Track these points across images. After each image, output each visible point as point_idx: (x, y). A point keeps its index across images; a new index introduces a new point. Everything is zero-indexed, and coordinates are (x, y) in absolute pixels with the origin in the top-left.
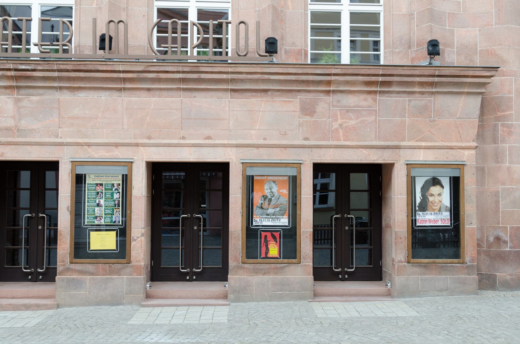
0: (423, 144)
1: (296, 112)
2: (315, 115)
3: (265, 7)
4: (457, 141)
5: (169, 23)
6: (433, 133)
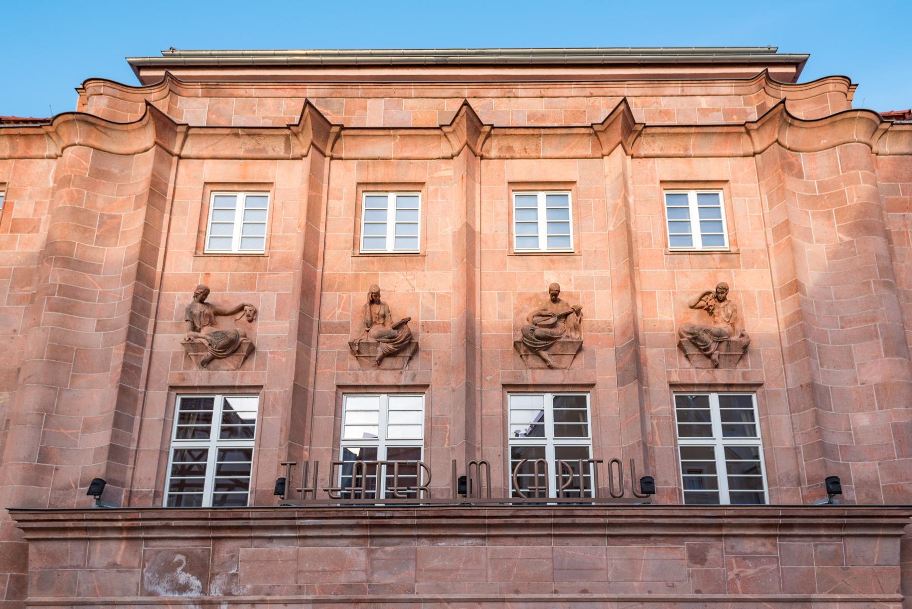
0: (838, 596)
1: (684, 559)
2: (706, 563)
3: (634, 444)
4: (878, 593)
5: (536, 463)
6: (848, 583)
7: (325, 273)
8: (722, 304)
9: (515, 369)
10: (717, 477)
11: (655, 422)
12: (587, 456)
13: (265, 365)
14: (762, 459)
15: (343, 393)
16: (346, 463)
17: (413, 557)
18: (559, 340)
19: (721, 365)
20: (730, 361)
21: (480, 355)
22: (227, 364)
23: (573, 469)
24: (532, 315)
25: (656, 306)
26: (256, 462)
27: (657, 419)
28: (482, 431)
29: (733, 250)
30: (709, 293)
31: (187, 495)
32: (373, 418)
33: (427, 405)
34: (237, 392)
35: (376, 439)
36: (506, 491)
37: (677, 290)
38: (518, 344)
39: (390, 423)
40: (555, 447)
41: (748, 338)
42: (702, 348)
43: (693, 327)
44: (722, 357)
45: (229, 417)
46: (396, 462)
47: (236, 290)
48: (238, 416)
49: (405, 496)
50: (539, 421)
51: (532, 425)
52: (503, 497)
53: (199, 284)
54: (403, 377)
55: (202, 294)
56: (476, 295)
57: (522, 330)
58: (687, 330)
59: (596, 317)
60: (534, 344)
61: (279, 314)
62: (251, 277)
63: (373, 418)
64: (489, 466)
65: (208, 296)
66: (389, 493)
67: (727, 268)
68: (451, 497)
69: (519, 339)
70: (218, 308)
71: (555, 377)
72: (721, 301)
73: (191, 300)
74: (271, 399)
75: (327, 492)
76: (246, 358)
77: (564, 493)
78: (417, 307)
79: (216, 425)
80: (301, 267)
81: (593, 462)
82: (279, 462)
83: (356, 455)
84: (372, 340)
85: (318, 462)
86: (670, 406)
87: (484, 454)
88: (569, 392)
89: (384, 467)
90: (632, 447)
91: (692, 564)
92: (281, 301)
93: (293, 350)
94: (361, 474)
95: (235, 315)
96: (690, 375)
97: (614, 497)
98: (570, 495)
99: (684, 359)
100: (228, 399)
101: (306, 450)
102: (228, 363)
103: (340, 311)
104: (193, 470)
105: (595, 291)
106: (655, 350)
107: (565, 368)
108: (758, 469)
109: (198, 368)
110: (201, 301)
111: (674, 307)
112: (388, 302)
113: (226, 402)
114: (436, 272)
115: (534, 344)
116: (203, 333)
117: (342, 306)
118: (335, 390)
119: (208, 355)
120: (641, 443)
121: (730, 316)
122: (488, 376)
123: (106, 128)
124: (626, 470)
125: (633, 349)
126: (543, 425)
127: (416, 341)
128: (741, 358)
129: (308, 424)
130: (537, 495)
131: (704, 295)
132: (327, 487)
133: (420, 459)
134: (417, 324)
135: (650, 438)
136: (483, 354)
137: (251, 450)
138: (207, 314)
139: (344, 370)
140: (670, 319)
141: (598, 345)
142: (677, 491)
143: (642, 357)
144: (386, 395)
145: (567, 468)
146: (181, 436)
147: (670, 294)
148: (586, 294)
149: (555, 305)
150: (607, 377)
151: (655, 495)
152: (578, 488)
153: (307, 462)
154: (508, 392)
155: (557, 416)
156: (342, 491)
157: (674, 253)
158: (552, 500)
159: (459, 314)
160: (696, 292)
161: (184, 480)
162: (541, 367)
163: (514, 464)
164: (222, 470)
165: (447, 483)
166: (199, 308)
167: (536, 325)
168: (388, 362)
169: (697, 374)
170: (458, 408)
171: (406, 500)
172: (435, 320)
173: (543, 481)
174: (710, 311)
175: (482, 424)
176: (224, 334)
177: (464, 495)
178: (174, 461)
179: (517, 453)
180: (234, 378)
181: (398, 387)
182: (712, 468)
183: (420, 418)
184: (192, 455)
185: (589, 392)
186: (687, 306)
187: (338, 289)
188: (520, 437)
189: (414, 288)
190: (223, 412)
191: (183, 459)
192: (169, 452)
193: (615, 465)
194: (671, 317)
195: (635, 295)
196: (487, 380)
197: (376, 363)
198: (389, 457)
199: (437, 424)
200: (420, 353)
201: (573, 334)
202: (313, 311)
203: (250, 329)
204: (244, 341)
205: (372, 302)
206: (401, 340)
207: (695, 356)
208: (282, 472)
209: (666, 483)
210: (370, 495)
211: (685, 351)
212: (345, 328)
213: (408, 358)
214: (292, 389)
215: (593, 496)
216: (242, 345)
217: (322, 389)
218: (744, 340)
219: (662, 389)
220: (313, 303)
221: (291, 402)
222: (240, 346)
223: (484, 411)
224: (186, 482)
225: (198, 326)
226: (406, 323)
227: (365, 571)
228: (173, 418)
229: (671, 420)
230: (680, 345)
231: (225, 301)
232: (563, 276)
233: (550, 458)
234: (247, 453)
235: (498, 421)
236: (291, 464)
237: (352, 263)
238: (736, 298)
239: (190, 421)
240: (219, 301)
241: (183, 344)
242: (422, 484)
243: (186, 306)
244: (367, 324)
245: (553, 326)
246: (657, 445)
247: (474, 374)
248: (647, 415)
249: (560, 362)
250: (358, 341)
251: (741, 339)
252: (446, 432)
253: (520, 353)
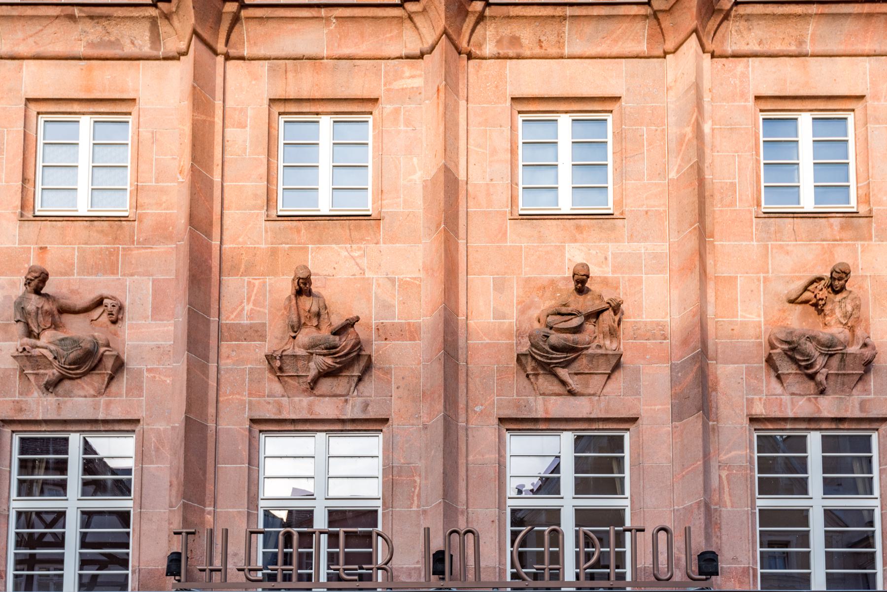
3: (691, 505)
5: (546, 533)
7: (224, 246)
8: (839, 297)
9: (517, 395)
10: (808, 531)
11: (724, 474)
12: (622, 523)
13: (140, 388)
14: (878, 528)
15: (261, 431)
16: (267, 532)
19: (829, 390)
20: (843, 384)
21: (464, 375)
22: (83, 388)
23: (600, 540)
24: (546, 314)
25: (737, 300)
26: (137, 530)
27: (728, 470)
28: (467, 486)
29: (863, 210)
30: (820, 279)
31: (40, 575)
32: (306, 467)
33: (386, 450)
34: (102, 429)
35: (310, 496)
36: (502, 572)
37: (770, 275)
38: (523, 359)
39: (331, 474)
40: (576, 510)
41: (874, 348)
42: (803, 364)
43: (791, 333)
44: (831, 378)
45: (92, 465)
46: (341, 530)
47: (89, 274)
48: (105, 463)
49: (356, 578)
50: (552, 473)
51: (541, 478)
52: (497, 580)
53: (31, 265)
54: (349, 407)
55: (36, 281)
56: (460, 282)
57: (529, 336)
58: (782, 336)
59: (644, 316)
60: (547, 358)
61: (157, 311)
62: (111, 254)
63: (306, 467)
64: (478, 537)
65: (47, 283)
66: (333, 573)
67: (851, 239)
68: (423, 580)
69: (524, 349)
70: (63, 301)
71: (579, 407)
72: (836, 292)
73: (21, 289)
74: (154, 439)
75: (242, 573)
76: (111, 378)
77: (586, 574)
78: (369, 300)
79: (74, 476)
80: (186, 237)
81: (630, 530)
82: (169, 529)
83: (282, 519)
84: (301, 352)
85: (227, 530)
86: (748, 451)
87: (470, 520)
88: (598, 429)
89: (324, 538)
90: (689, 510)
92: (158, 291)
93: (181, 366)
94: (291, 547)
95: (90, 313)
96: (781, 404)
97: (658, 579)
98: (596, 576)
99: (774, 381)
100: (88, 439)
101: (209, 513)
102: (85, 386)
103: (251, 306)
104: (46, 539)
105: (644, 276)
106: (731, 367)
107: (594, 395)
108: (871, 541)
109: (40, 393)
110: (37, 291)
111: (764, 302)
112: (325, 293)
113: (86, 442)
114: (398, 245)
115: (547, 358)
116: (44, 340)
117: (253, 298)
118: (248, 426)
119: (53, 374)
120: (702, 504)
121: (848, 314)
122: (477, 405)
124: (679, 543)
125: (697, 365)
126: (559, 478)
127: (368, 353)
128: (860, 379)
129: (210, 475)
130: (547, 576)
131: (812, 283)
132: (241, 565)
133: (377, 527)
134: (369, 327)
135: (716, 498)
136: (470, 374)
137: (128, 513)
138: (47, 312)
139: (260, 396)
140: (758, 319)
141: (644, 358)
142: (751, 571)
143: (711, 377)
144: (324, 434)
145: (591, 538)
146: (23, 492)
147: (759, 280)
148: (629, 280)
149: (581, 298)
150: (657, 407)
151: (719, 577)
152: (608, 567)
153: (211, 530)
154: (507, 430)
155: (580, 465)
156: (265, 571)
157: (769, 215)
158: (569, 584)
159: (433, 312)
160: (799, 278)
161: (34, 554)
162: (557, 392)
163: (514, 534)
164: (88, 540)
165: (416, 560)
166: (34, 303)
167: (551, 328)
168: (326, 385)
169: (792, 403)
170: (433, 452)
171: (358, 583)
172: (396, 321)
173: (556, 558)
174: (818, 307)
175: (467, 477)
176: (76, 342)
177: (441, 576)
178: (17, 528)
179: (519, 518)
180: (96, 408)
181: (343, 421)
182: (804, 538)
183: (375, 467)
184: (41, 519)
185: (628, 430)
186: (785, 299)
187: (246, 273)
188: (523, 495)
189: (364, 270)
190: (84, 459)
191: (30, 525)
192: (8, 516)
193: (662, 535)
194: (759, 316)
195: (706, 281)
196: (475, 412)
197: (308, 386)
198: (331, 524)
199: (401, 476)
200: (374, 371)
201: (608, 342)
202: (210, 306)
203: (115, 334)
204: (107, 353)
205: (299, 293)
206: (345, 351)
207: (791, 376)
208: (176, 543)
209: (735, 559)
210: (305, 577)
211: (776, 369)
212: (259, 334)
213: (356, 379)
214: (184, 424)
215: (629, 578)
216: (104, 359)
217: (228, 425)
218: (867, 352)
219: (738, 426)
220: (208, 293)
221: (183, 444)
222: (100, 360)
223: (471, 458)
224: (38, 557)
225: (36, 330)
226: (352, 326)
228: (10, 467)
229: (749, 471)
230: (769, 360)
231: (72, 292)
232: (594, 252)
233: (568, 526)
234: (124, 517)
235: (492, 473)
236: (188, 533)
237: (266, 232)
238: (860, 287)
239: (36, 471)
240: (65, 291)
241: (14, 357)
242: (380, 561)
243: (14, 299)
244: (293, 327)
245: (577, 330)
246: (726, 507)
247: (455, 403)
248: (714, 464)
249: (587, 385)
250: (279, 353)
251: (863, 350)
252: (415, 487)
253: (525, 372)
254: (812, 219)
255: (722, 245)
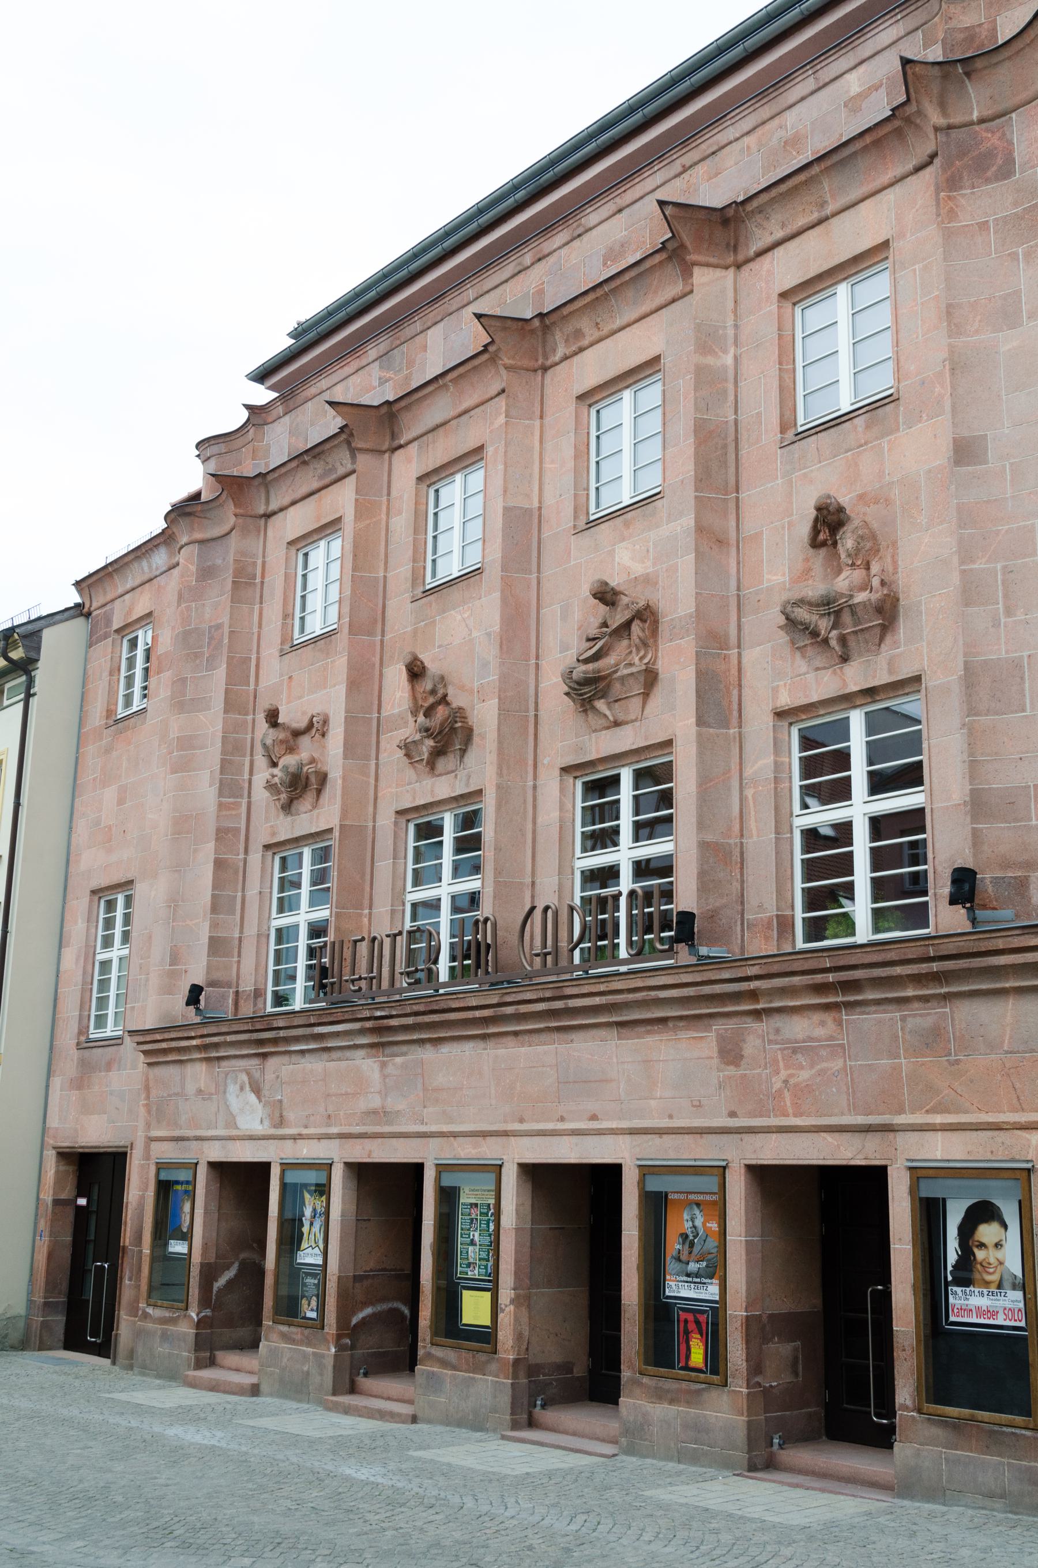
0: (938, 1119)
1: (713, 1058)
2: (742, 1063)
4: (1014, 1110)
6: (959, 1091)
17: (420, 1071)
18: (615, 676)
91: (723, 1066)
111: (789, 555)
123: (202, 511)
222: (307, 778)
227: (380, 1092)
232: (638, 547)
254: (835, 428)
255: (749, 495)
